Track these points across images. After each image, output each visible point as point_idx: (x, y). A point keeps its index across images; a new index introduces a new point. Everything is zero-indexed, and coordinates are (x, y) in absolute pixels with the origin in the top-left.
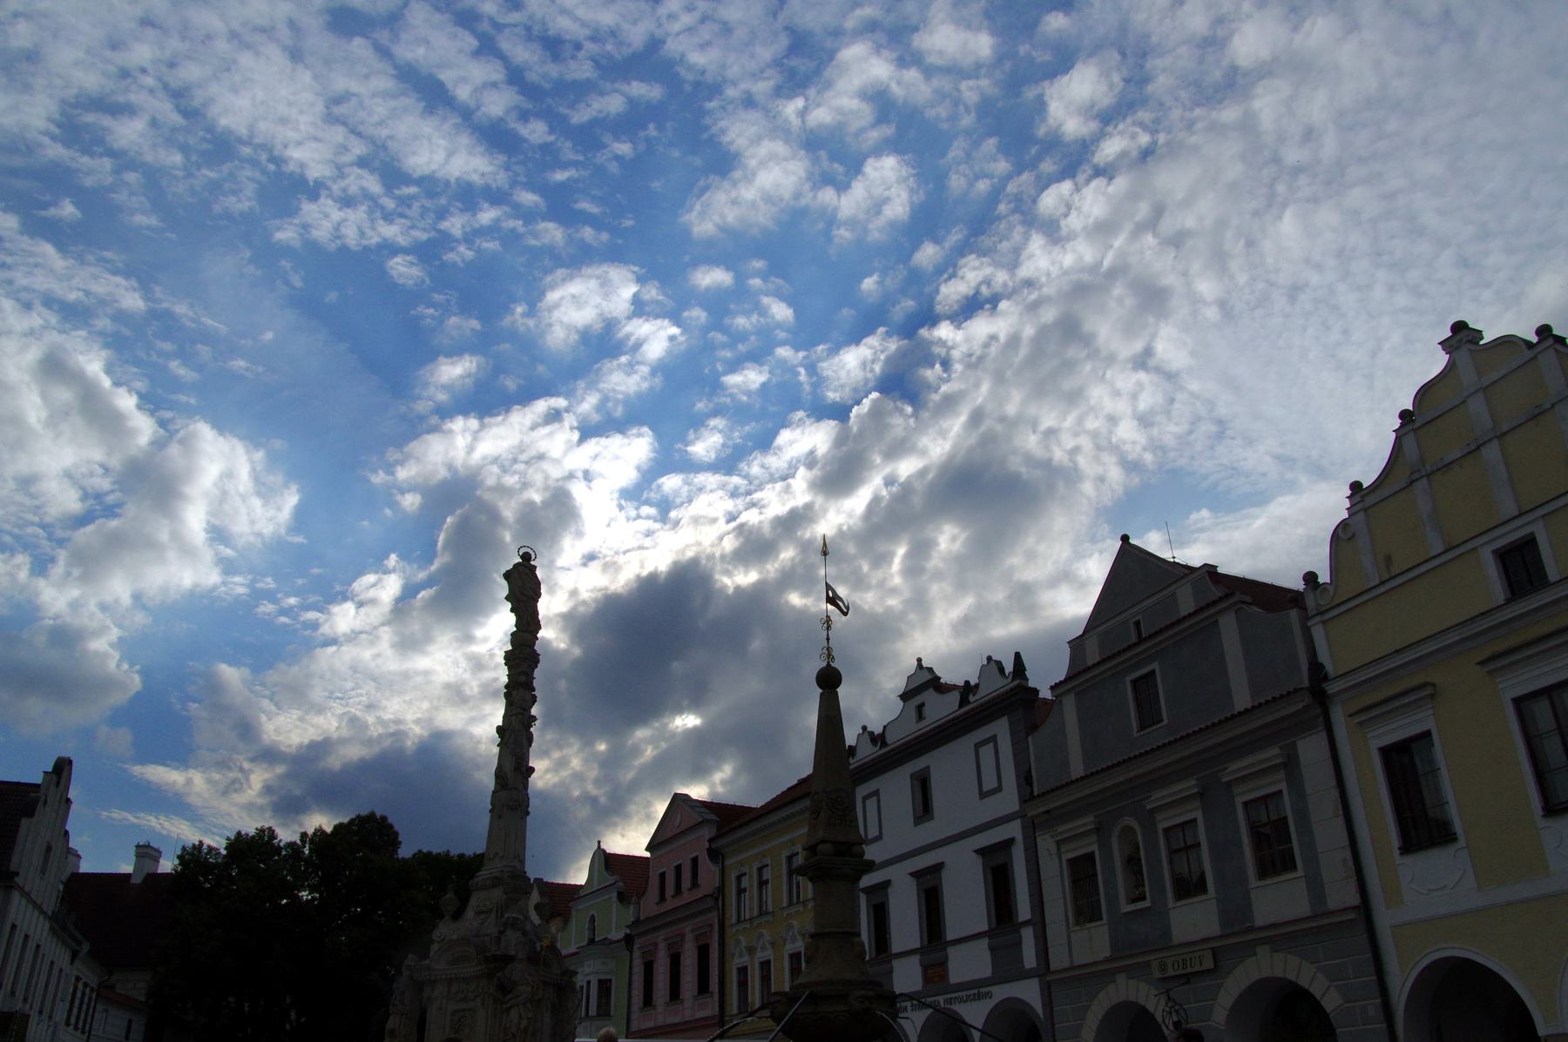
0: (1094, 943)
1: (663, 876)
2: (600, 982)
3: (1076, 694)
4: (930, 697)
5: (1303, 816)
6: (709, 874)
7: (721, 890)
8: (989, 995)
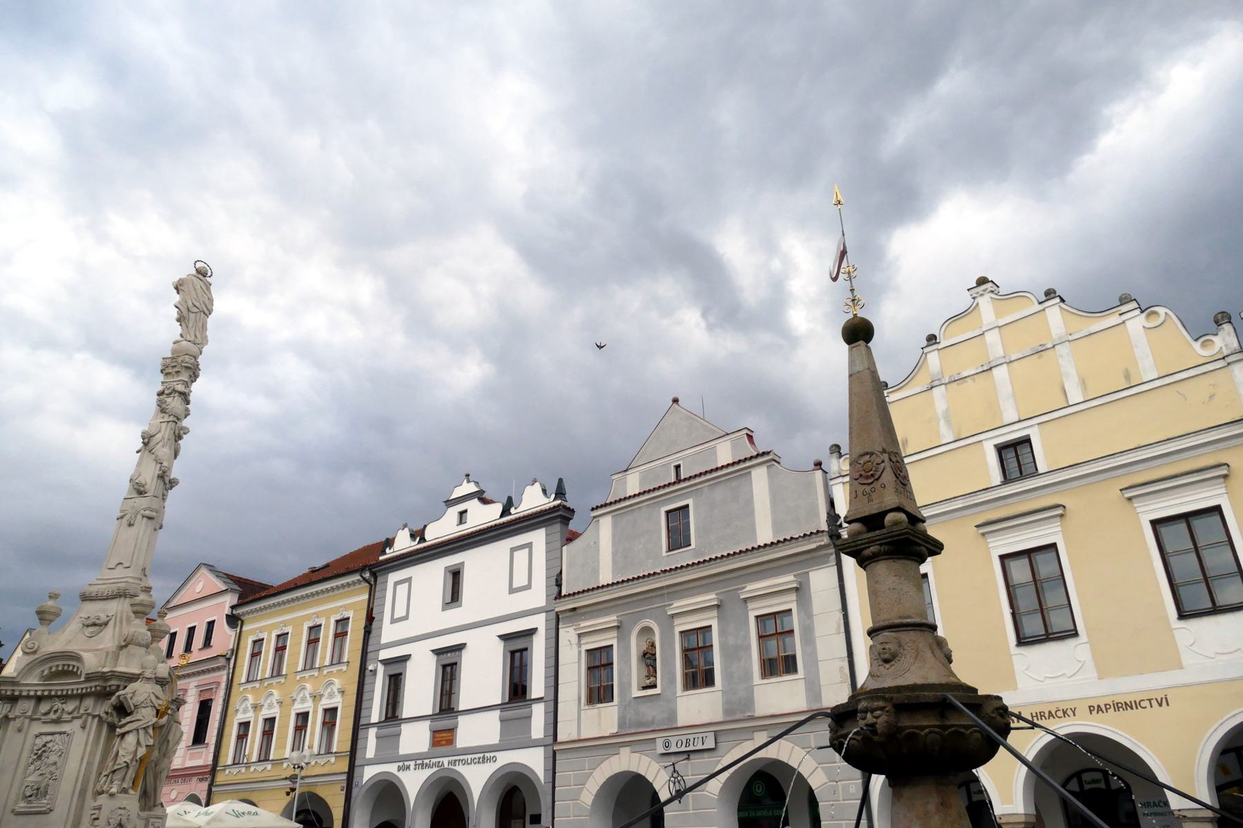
0: (604, 720)
3: (613, 516)
4: (473, 506)
5: (808, 631)
6: (224, 637)
7: (236, 651)
8: (494, 759)
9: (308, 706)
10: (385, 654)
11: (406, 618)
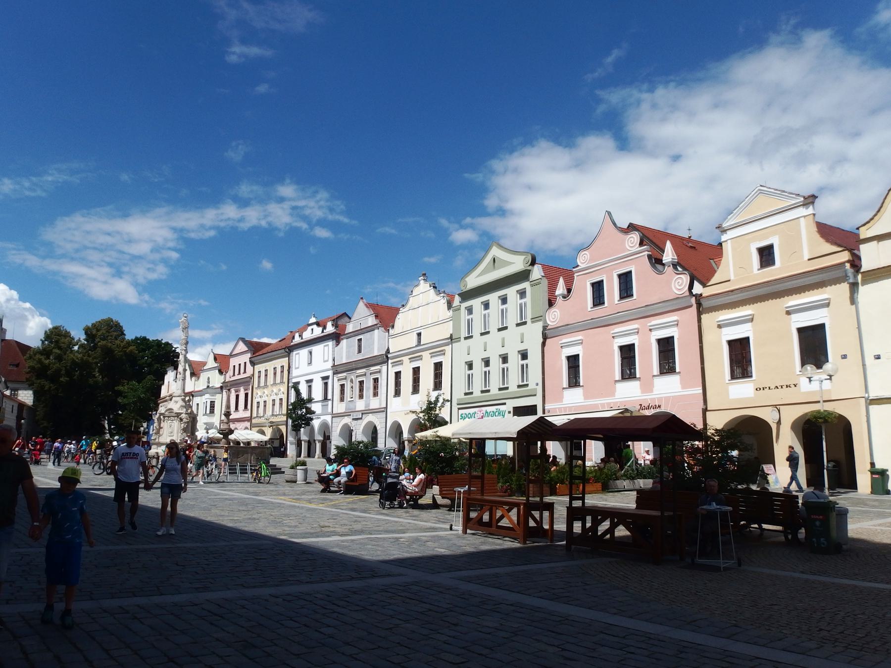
1: (234, 366)
2: (211, 402)
4: (315, 327)
6: (249, 367)
7: (253, 375)
8: (320, 418)
9: (274, 397)
10: (294, 380)
11: (298, 368)
